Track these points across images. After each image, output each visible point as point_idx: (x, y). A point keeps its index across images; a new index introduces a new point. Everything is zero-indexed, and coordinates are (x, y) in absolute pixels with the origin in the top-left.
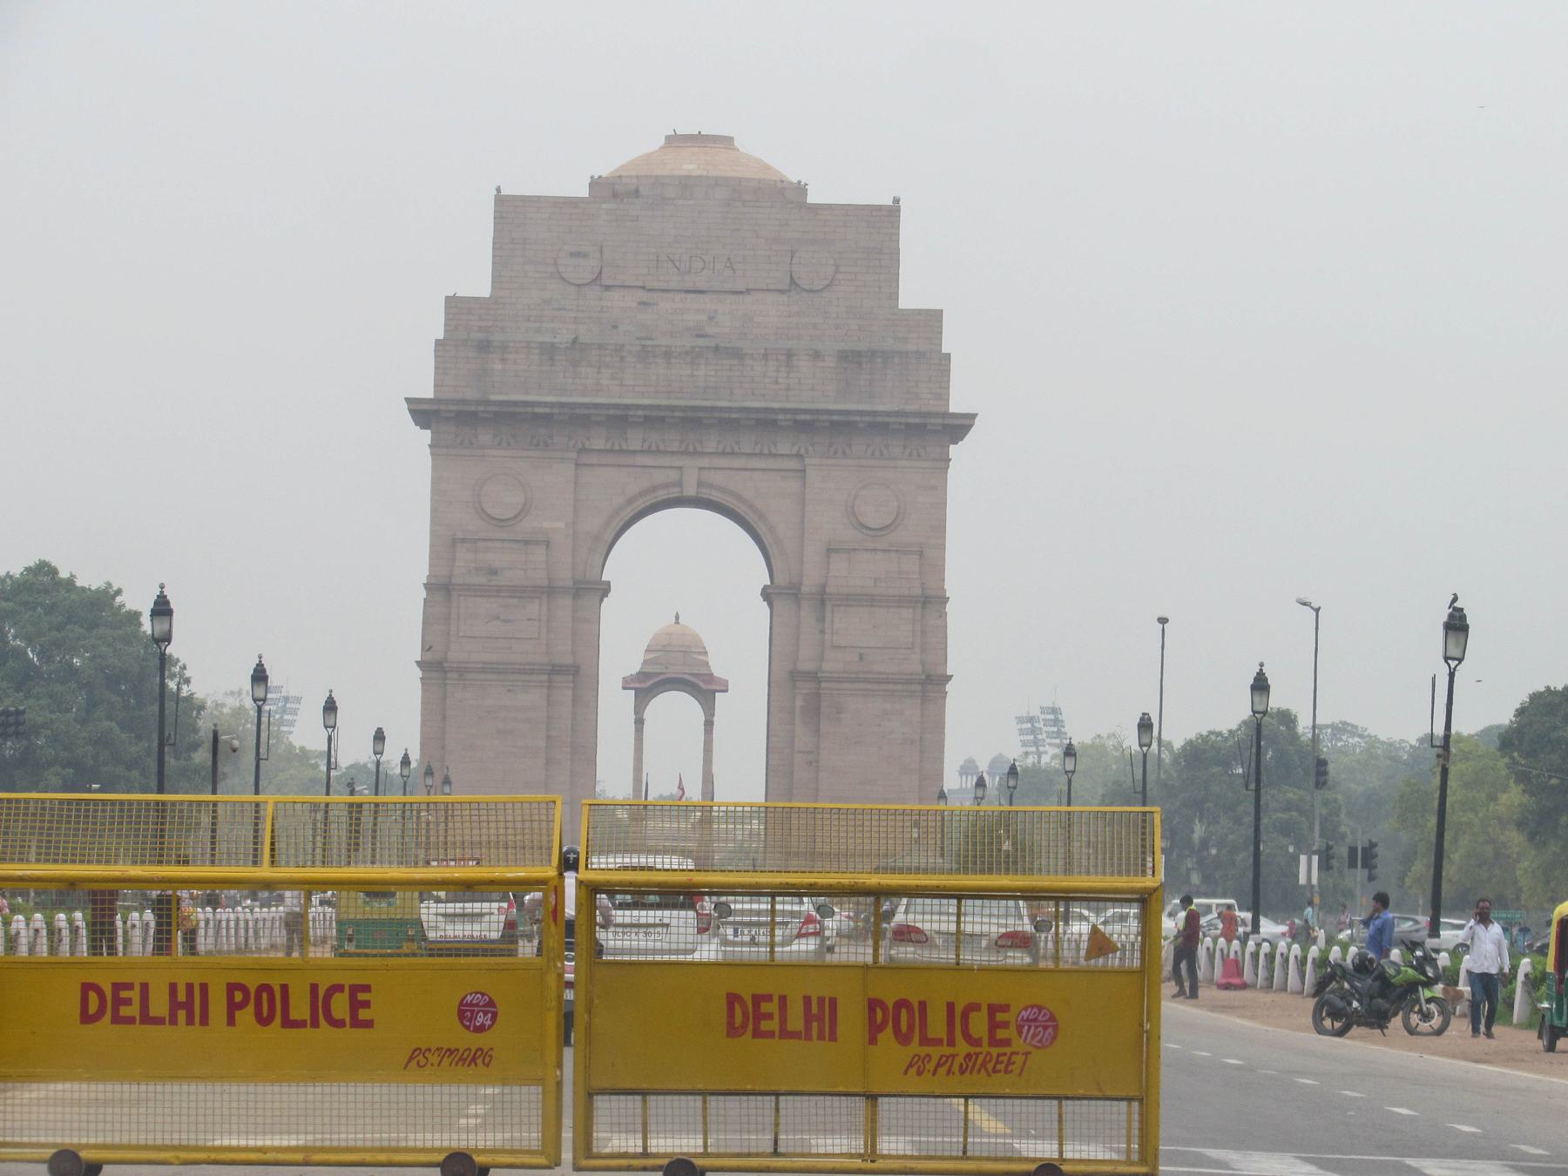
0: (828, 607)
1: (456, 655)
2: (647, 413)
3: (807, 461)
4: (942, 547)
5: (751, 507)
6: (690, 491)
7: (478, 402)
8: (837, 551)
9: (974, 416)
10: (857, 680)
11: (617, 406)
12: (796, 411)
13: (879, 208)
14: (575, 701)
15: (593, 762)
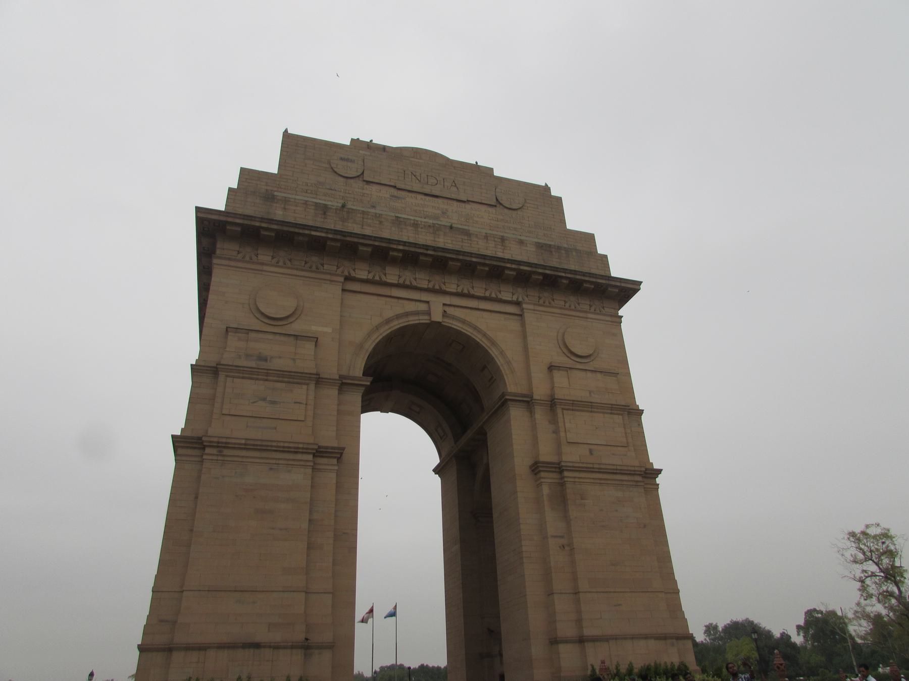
0: (559, 411)
1: (217, 430)
2: (406, 248)
3: (524, 306)
4: (628, 374)
5: (484, 335)
6: (437, 317)
7: (262, 220)
8: (558, 368)
9: (640, 283)
10: (591, 470)
11: (382, 239)
12: (519, 263)
13: (539, 186)
14: (339, 486)
15: (353, 549)
